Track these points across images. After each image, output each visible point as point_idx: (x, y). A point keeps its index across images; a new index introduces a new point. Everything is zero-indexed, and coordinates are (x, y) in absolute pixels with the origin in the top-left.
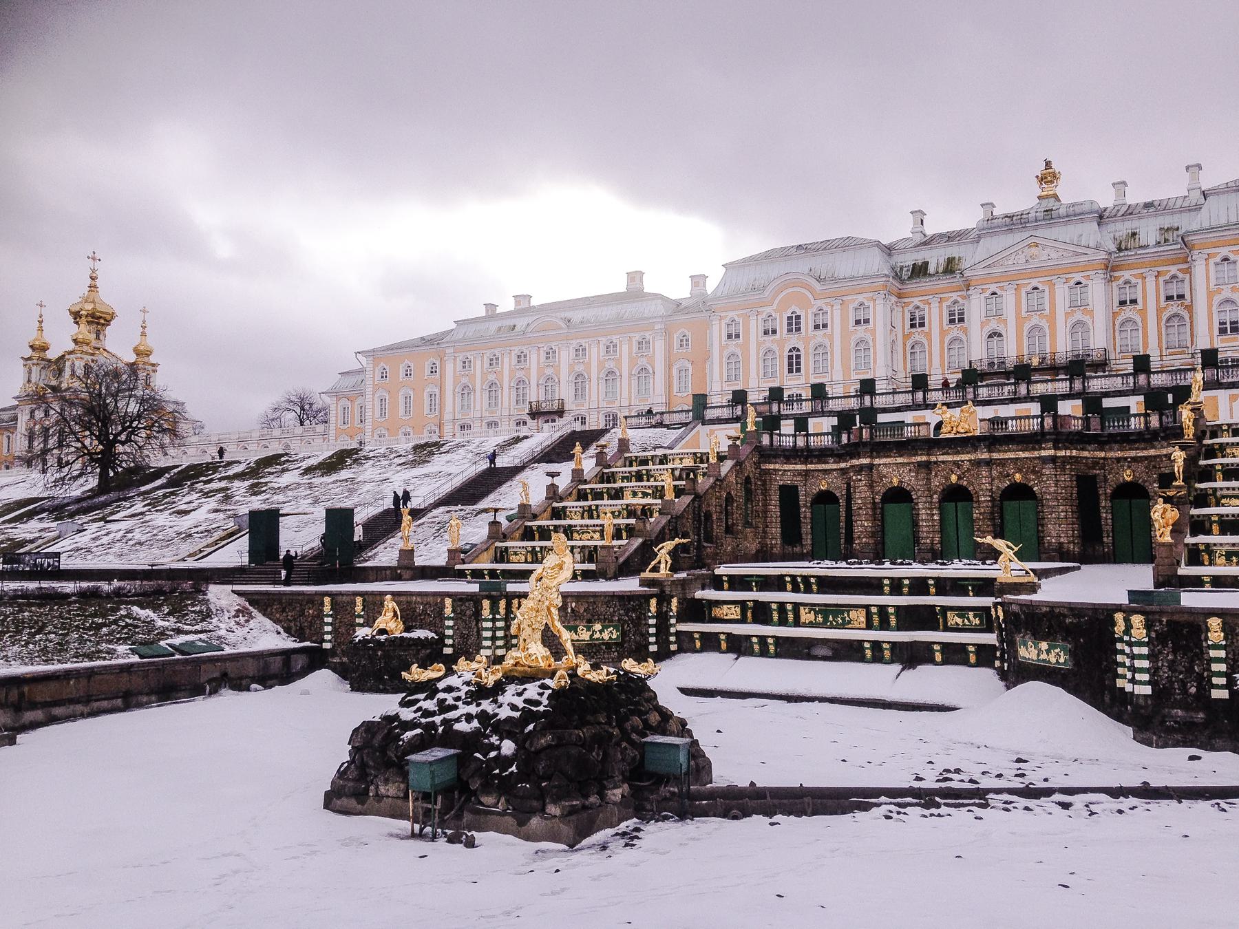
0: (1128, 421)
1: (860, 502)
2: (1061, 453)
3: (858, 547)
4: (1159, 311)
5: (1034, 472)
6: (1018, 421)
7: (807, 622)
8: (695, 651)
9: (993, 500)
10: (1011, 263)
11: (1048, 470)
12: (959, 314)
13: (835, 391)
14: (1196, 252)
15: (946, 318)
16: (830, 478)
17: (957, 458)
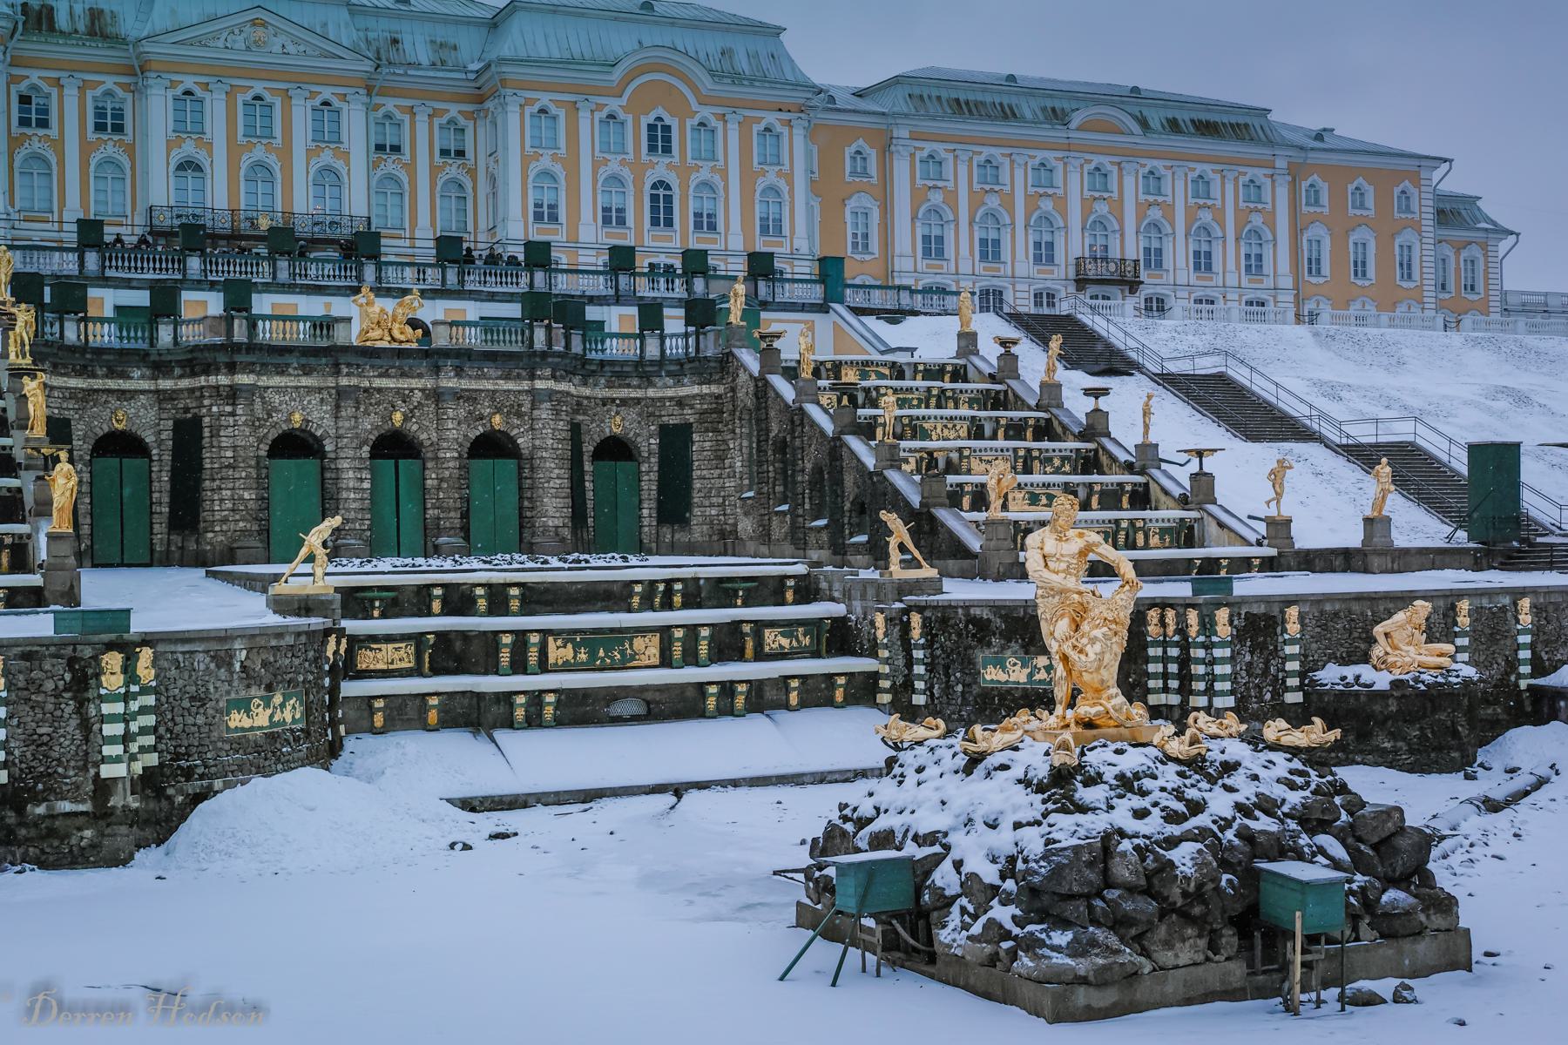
0: (603, 342)
1: (229, 454)
2: (562, 386)
3: (220, 538)
4: (434, 171)
5: (519, 415)
6: (288, 323)
7: (560, 662)
8: (427, 728)
9: (460, 456)
10: (220, 44)
11: (544, 412)
12: (114, 116)
13: (730, 267)
14: (509, 91)
15: (90, 121)
16: (131, 408)
17: (404, 384)
